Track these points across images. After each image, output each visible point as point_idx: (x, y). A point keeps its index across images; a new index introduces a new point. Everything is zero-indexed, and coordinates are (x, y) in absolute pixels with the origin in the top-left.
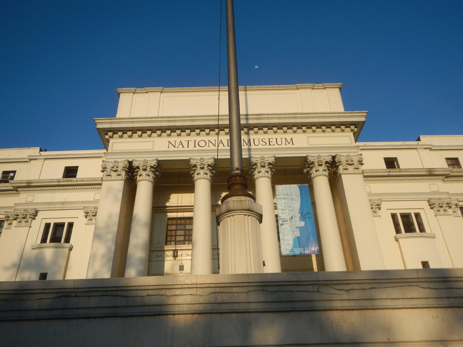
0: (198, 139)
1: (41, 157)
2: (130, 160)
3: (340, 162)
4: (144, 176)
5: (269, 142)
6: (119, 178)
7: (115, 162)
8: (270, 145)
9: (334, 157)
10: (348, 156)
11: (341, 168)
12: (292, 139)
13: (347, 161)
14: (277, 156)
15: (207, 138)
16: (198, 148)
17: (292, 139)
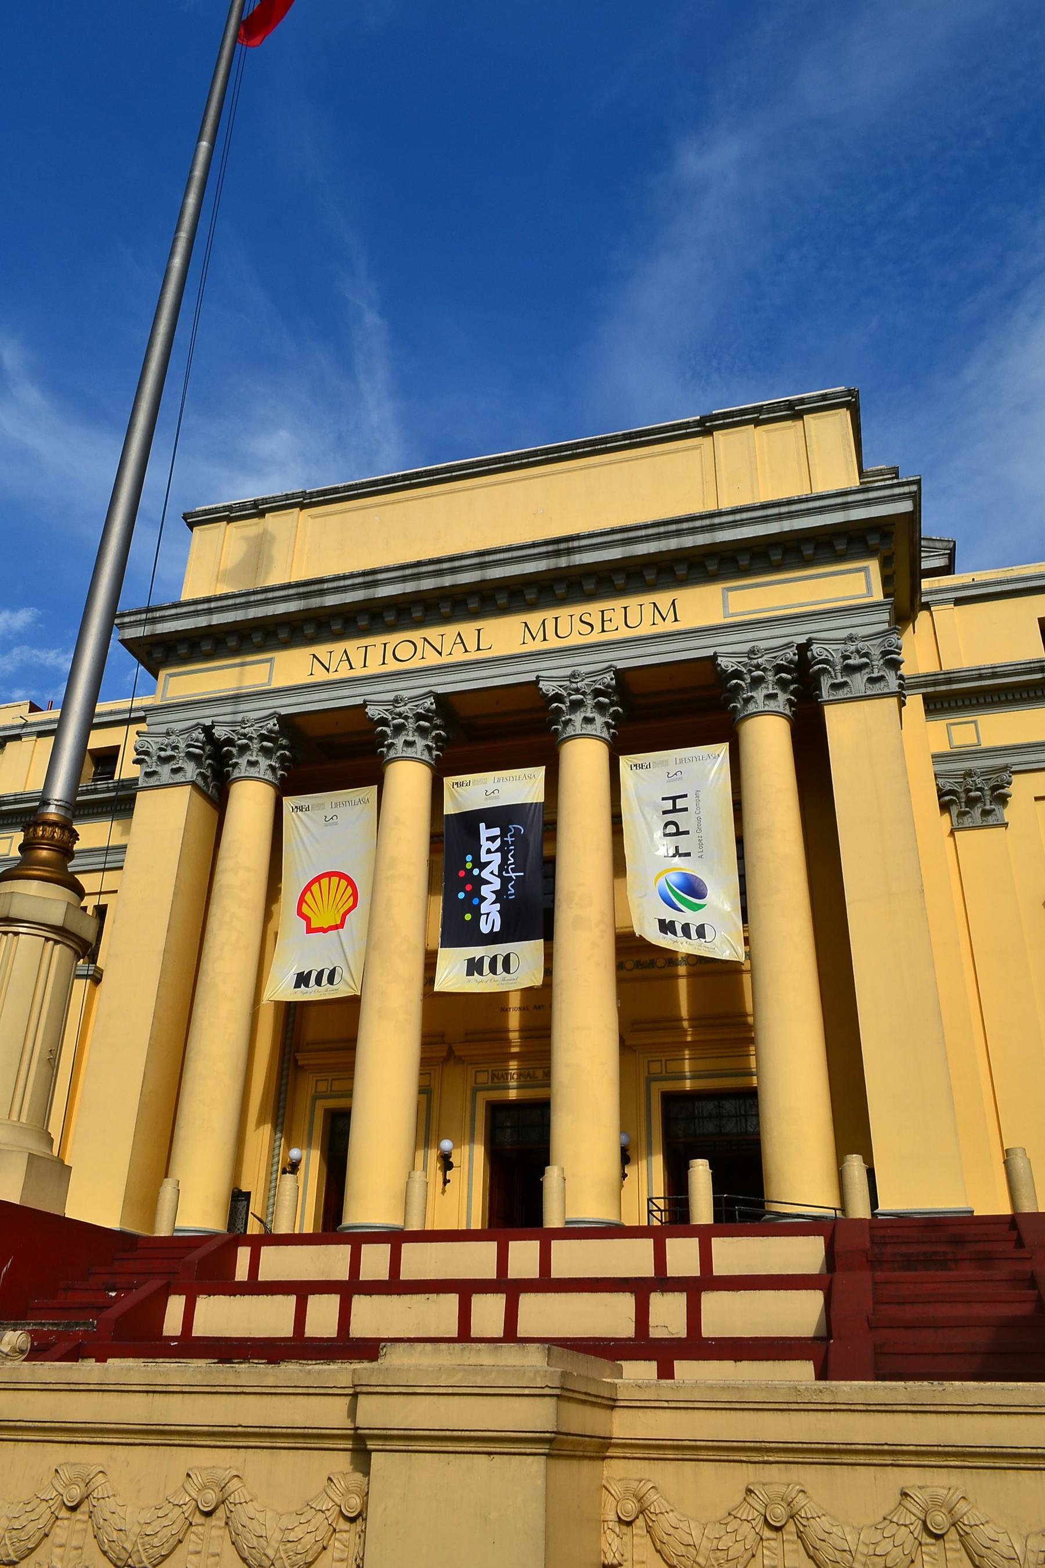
0: (393, 639)
1: (29, 730)
2: (208, 722)
3: (826, 661)
4: (243, 770)
5: (603, 621)
6: (179, 778)
7: (168, 734)
8: (603, 631)
9: (803, 649)
10: (851, 639)
11: (826, 683)
12: (673, 603)
13: (846, 657)
14: (620, 665)
15: (416, 635)
16: (393, 666)
17: (673, 603)
